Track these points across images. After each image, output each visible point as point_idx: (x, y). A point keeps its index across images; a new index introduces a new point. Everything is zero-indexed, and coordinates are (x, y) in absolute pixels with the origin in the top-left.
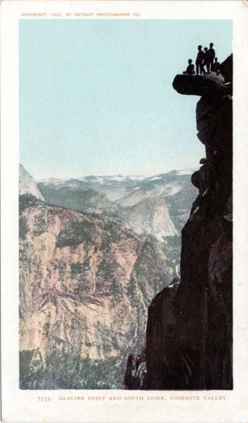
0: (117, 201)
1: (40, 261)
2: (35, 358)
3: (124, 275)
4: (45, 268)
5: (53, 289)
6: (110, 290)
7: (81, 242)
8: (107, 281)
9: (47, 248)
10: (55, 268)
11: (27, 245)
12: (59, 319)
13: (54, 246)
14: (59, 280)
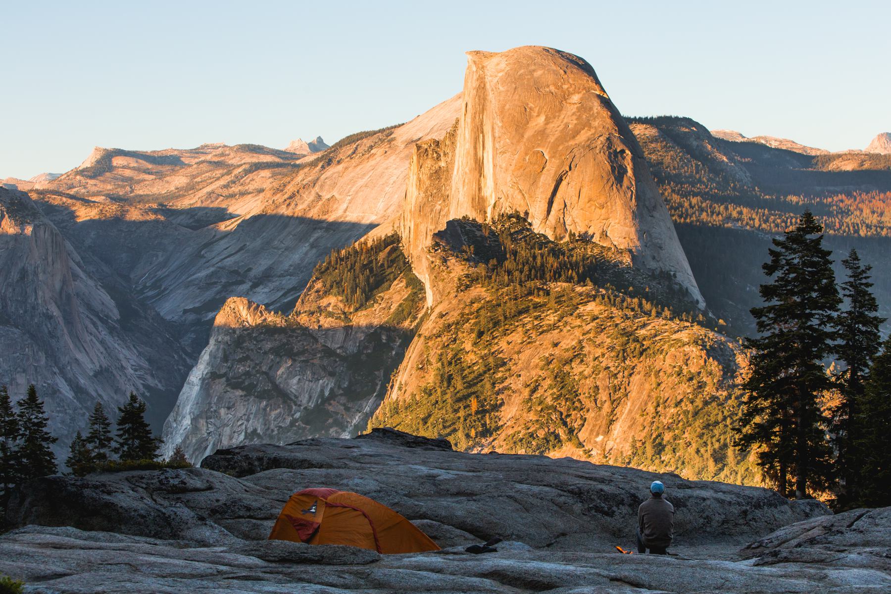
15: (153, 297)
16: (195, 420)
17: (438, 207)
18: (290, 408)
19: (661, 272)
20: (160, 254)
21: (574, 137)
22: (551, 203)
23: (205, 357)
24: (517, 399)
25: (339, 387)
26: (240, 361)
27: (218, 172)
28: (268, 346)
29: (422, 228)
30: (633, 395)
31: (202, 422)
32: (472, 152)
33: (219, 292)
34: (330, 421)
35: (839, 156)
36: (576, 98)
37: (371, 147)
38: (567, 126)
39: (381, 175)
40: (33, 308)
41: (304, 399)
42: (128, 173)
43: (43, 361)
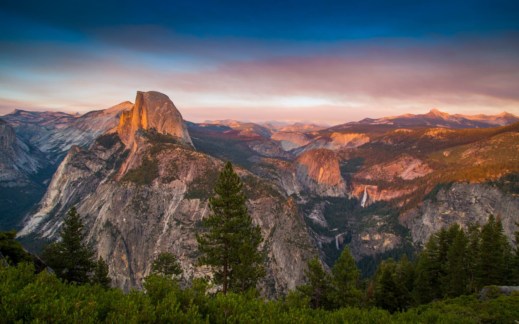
0: (293, 150)
1: (162, 215)
4: (166, 222)
5: (169, 248)
9: (174, 198)
10: (178, 224)
15: (37, 146)
16: (63, 175)
17: (128, 126)
18: (90, 172)
19: (188, 143)
20: (38, 136)
21: (167, 112)
22: (162, 126)
23: (66, 159)
24: (163, 169)
25: (104, 167)
26: (76, 160)
27: (52, 118)
28: (84, 157)
29: (124, 131)
31: (65, 175)
32: (138, 114)
33: (57, 146)
34: (102, 175)
35: (201, 124)
36: (166, 103)
37: (98, 114)
38: (165, 109)
39: (101, 121)
40: (6, 147)
41: (94, 170)
42: (25, 116)
43: (9, 160)
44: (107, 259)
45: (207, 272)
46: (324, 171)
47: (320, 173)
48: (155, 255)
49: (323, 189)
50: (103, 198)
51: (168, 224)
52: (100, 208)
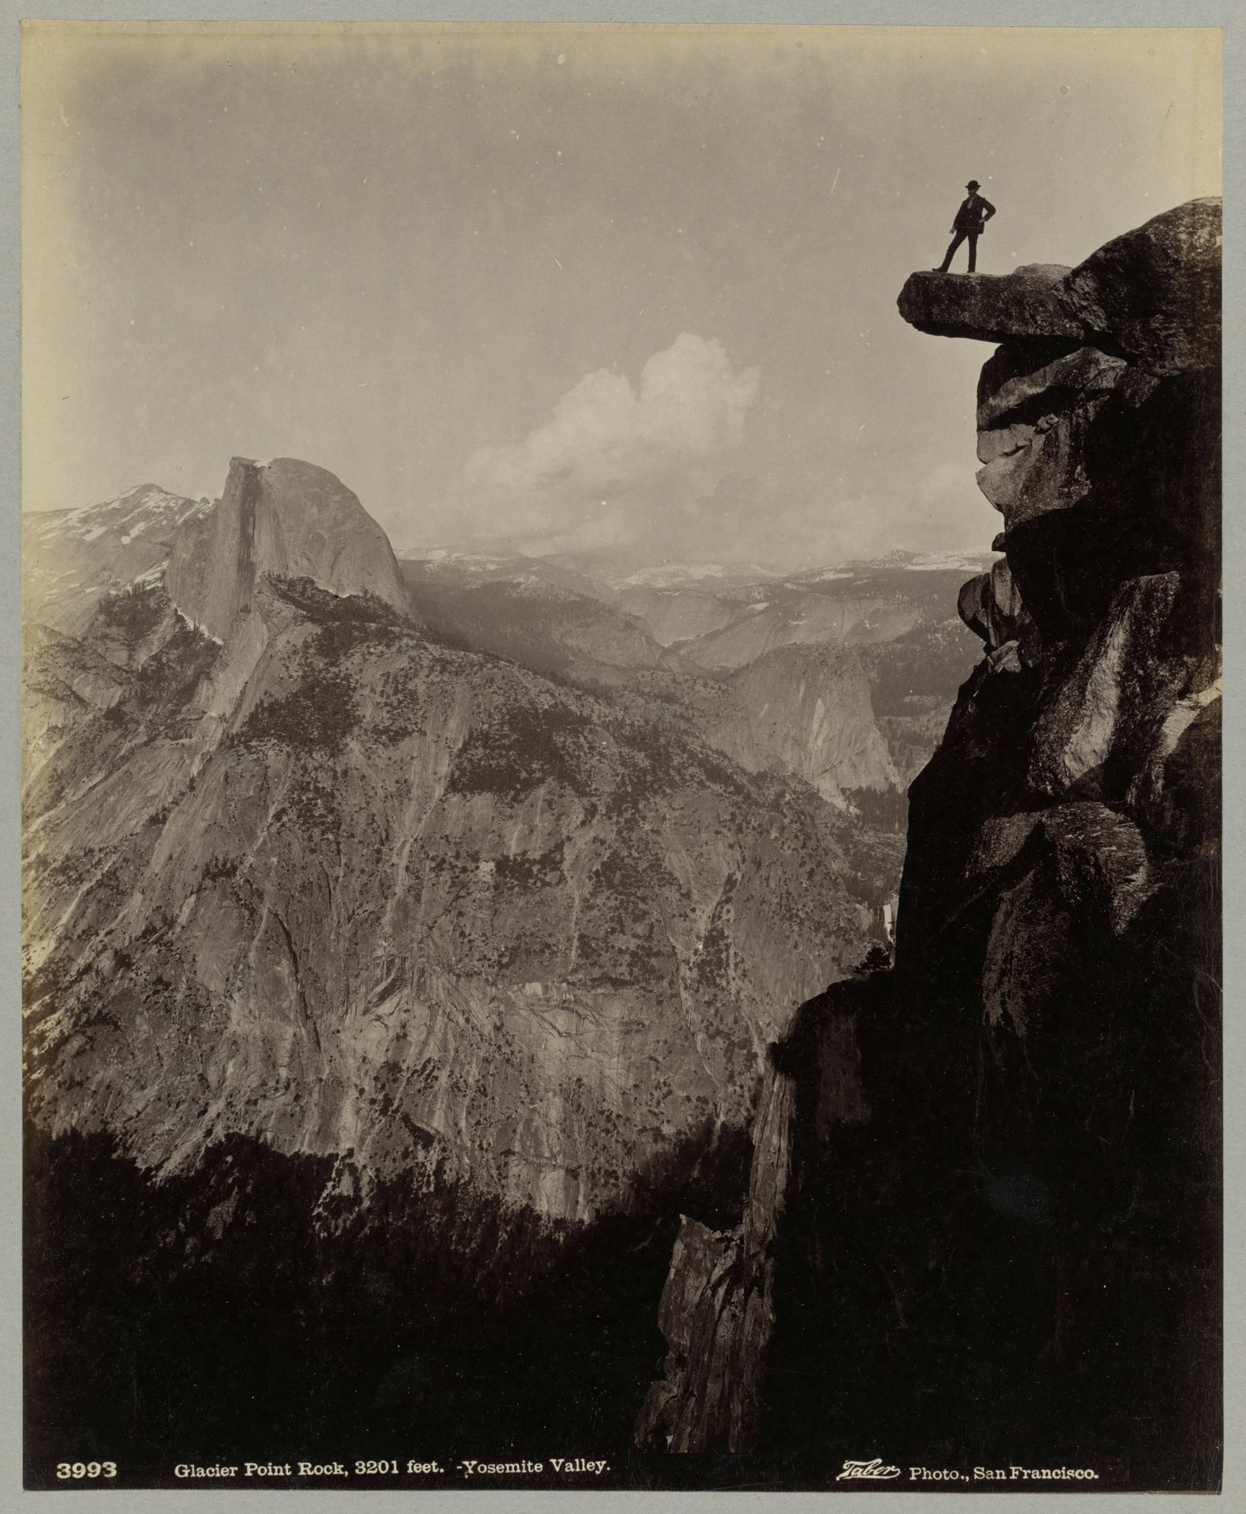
1: (386, 839)
2: (334, 1187)
3: (657, 1069)
4: (403, 863)
5: (421, 942)
6: (629, 965)
7: (541, 781)
8: (622, 932)
9: (415, 792)
10: (439, 868)
11: (345, 773)
12: (432, 1052)
13: (439, 791)
14: (447, 911)
29: (188, 581)
30: (458, 697)
34: (128, 718)
44: (228, 974)
45: (545, 1008)
46: (827, 711)
47: (816, 716)
48: (378, 961)
49: (823, 766)
50: (152, 792)
51: (407, 869)
52: (157, 821)
